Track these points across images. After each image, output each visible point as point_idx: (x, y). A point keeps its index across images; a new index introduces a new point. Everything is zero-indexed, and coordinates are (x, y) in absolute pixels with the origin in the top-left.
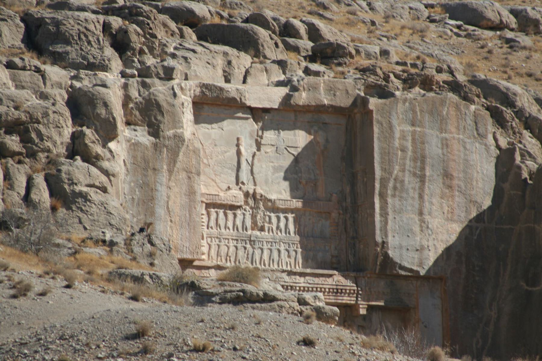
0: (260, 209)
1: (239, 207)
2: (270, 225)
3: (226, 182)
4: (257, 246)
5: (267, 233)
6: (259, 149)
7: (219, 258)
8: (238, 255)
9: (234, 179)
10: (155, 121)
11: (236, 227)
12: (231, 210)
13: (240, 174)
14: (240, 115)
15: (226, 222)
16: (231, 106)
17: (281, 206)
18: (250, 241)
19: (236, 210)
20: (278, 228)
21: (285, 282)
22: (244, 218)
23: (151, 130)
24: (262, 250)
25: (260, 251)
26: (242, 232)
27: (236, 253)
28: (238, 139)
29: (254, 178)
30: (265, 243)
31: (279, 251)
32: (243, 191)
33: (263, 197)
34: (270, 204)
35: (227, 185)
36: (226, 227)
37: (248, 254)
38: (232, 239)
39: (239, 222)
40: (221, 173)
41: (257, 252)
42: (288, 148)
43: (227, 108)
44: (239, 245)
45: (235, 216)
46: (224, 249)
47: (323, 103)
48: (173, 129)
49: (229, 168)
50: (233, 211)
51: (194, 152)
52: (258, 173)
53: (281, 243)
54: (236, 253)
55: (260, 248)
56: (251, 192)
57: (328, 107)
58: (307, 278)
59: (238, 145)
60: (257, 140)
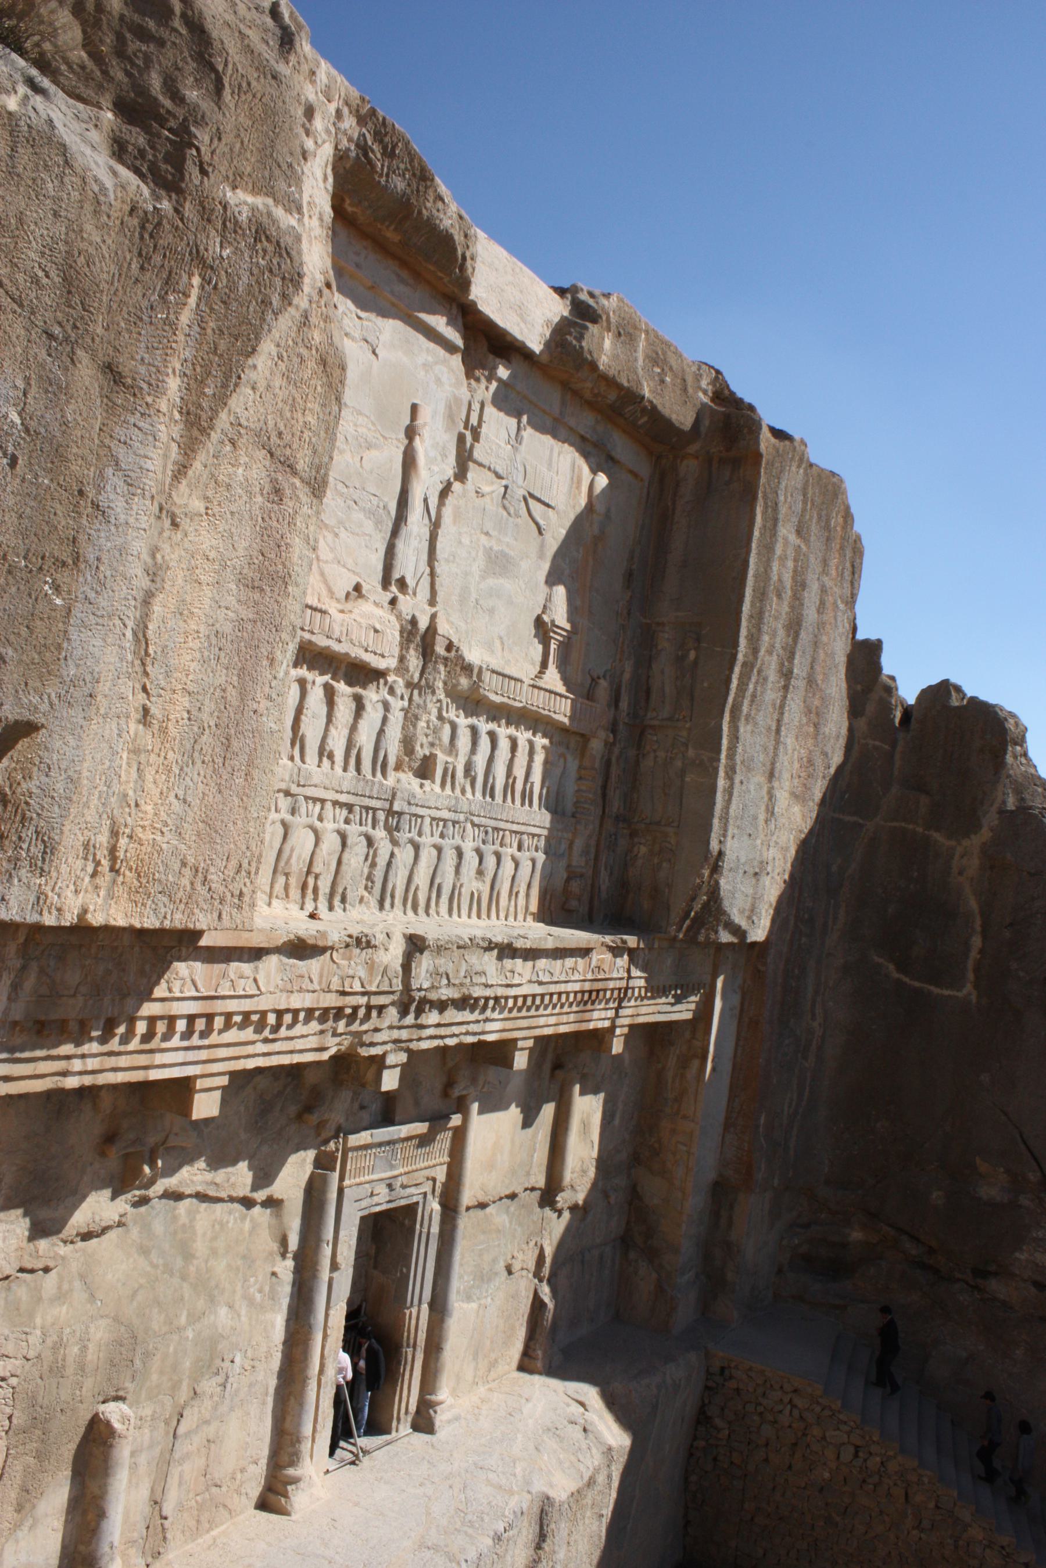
0: (434, 693)
1: (377, 675)
2: (450, 760)
3: (350, 563)
4: (403, 836)
5: (437, 788)
6: (461, 475)
7: (281, 880)
8: (344, 868)
9: (377, 561)
10: (168, 103)
11: (354, 752)
12: (350, 684)
13: (400, 545)
14: (439, 322)
15: (327, 730)
16: (417, 275)
17: (493, 697)
18: (390, 812)
19: (364, 686)
20: (468, 768)
21: (487, 986)
22: (385, 720)
23: (138, 138)
24: (417, 847)
25: (410, 849)
26: (369, 777)
27: (339, 862)
28: (414, 408)
29: (433, 574)
30: (427, 820)
31: (460, 855)
32: (399, 617)
33: (453, 653)
34: (464, 682)
35: (356, 579)
36: (324, 752)
37: (373, 865)
38: (335, 803)
39: (366, 738)
40: (341, 522)
41: (405, 855)
42: (530, 501)
43: (405, 274)
44: (353, 830)
45: (360, 706)
46: (302, 842)
47: (642, 393)
48: (255, 191)
49: (370, 513)
50: (358, 690)
51: (323, 362)
52: (447, 561)
53: (469, 826)
54: (339, 862)
55: (411, 842)
56: (423, 624)
57: (644, 410)
58: (542, 963)
59: (411, 432)
60: (461, 438)
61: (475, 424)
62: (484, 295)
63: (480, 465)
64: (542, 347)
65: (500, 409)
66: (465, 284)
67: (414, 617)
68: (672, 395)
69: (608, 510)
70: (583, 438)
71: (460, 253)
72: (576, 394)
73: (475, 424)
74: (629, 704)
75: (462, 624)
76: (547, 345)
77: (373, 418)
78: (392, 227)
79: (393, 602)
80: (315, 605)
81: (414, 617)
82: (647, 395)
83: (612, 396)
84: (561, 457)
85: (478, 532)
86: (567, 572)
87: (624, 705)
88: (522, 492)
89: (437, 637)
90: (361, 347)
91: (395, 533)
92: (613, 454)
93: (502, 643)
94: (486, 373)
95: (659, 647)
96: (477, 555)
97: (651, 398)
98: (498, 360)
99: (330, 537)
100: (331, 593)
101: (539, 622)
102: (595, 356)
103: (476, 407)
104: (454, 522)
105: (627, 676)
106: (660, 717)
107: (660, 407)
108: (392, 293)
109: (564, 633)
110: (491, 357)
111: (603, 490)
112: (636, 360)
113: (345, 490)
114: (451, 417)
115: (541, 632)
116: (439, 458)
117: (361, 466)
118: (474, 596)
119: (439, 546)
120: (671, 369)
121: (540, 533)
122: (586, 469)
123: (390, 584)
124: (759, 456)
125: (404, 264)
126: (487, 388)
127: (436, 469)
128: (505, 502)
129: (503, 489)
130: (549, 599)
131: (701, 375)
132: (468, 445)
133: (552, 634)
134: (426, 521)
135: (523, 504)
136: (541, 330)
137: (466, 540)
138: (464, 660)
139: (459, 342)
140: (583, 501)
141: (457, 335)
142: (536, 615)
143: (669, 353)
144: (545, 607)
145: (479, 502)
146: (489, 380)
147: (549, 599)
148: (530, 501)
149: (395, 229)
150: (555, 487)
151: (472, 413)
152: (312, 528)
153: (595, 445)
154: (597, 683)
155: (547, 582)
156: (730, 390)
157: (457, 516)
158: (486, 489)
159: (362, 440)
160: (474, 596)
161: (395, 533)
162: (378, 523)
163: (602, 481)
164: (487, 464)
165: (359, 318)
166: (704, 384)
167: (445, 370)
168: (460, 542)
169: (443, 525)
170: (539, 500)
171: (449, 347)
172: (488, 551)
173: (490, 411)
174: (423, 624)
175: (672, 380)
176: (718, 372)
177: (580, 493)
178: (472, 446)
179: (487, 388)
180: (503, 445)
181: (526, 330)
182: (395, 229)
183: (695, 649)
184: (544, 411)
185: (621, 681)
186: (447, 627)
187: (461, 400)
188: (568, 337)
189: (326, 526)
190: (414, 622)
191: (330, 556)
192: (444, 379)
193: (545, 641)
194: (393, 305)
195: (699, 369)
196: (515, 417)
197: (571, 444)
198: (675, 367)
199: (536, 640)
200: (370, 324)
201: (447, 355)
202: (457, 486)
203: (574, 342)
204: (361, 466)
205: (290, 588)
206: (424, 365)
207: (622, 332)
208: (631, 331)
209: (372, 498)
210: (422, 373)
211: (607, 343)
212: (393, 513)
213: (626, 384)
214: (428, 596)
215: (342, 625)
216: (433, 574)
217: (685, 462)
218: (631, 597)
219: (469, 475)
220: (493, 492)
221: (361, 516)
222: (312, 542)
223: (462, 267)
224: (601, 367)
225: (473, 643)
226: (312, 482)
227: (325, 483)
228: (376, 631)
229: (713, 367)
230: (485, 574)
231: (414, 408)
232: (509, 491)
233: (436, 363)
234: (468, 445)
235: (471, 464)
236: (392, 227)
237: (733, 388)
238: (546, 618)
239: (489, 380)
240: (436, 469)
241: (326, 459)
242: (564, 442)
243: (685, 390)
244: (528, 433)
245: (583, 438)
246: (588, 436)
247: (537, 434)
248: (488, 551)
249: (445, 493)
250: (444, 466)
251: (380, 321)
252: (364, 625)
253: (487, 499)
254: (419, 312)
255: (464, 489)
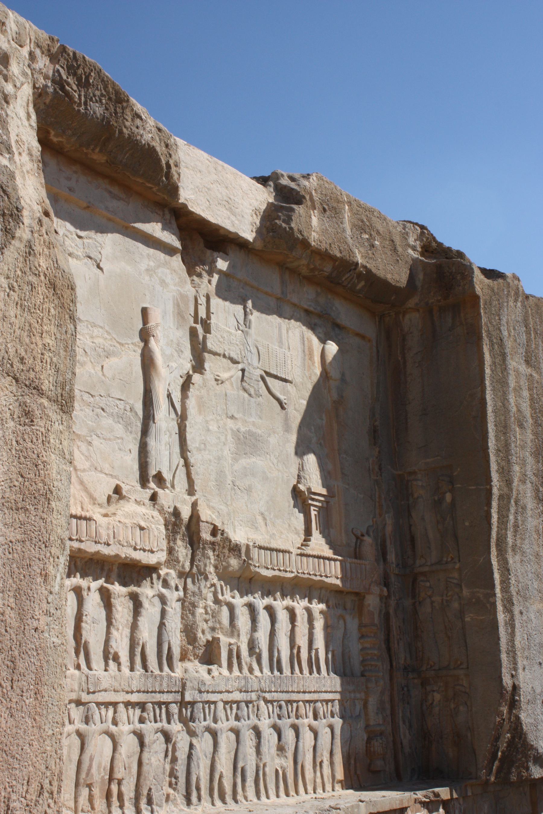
0: (206, 578)
2: (233, 641)
3: (106, 467)
4: (199, 726)
5: (225, 672)
11: (138, 650)
12: (124, 584)
13: (152, 442)
15: (108, 632)
17: (265, 573)
18: (183, 704)
20: (252, 646)
22: (163, 613)
24: (214, 734)
25: (208, 737)
26: (157, 672)
27: (140, 764)
28: (145, 312)
29: (187, 465)
30: (220, 705)
32: (161, 511)
33: (219, 537)
34: (234, 563)
35: (113, 483)
37: (174, 760)
38: (128, 704)
40: (92, 431)
42: (268, 379)
43: (116, 190)
44: (149, 728)
47: (355, 261)
49: (120, 417)
50: (133, 588)
51: (53, 286)
52: (199, 449)
53: (262, 703)
54: (140, 764)
55: (208, 729)
56: (186, 514)
57: (360, 275)
60: (193, 333)
61: (204, 316)
62: (192, 197)
63: (215, 354)
64: (254, 235)
65: (225, 299)
66: (174, 190)
67: (175, 508)
68: (383, 256)
69: (343, 375)
70: (307, 312)
71: (164, 162)
72: (294, 272)
73: (204, 316)
74: (397, 555)
75: (223, 507)
76: (259, 232)
77: (107, 328)
78: (97, 150)
79: (154, 498)
80: (79, 514)
81: (175, 508)
82: (360, 261)
83: (328, 268)
84: (290, 332)
85: (224, 417)
86: (314, 440)
87: (392, 557)
88: (259, 372)
89: (201, 524)
90: (86, 264)
91: (145, 432)
92: (338, 321)
93: (265, 519)
94: (207, 268)
95: (416, 495)
96: (226, 439)
97: (365, 263)
98: (215, 254)
99: (84, 447)
100: (93, 500)
101: (296, 492)
102: (305, 234)
103: (202, 300)
104: (200, 412)
105: (389, 529)
106: (429, 563)
107: (374, 270)
108: (107, 208)
109: (322, 499)
110: (209, 252)
111: (335, 357)
112: (344, 230)
113: (92, 399)
114: (180, 315)
115: (299, 502)
116: (175, 354)
117: (104, 375)
118: (229, 479)
119: (189, 436)
120: (378, 233)
121: (283, 408)
122: (315, 340)
123: (148, 481)
124: (477, 298)
125: (113, 181)
126: (210, 282)
127: (174, 365)
128: (244, 384)
129: (240, 373)
130: (301, 468)
131: (407, 234)
132: (201, 337)
133: (310, 502)
134: (173, 415)
135: (261, 383)
136: (251, 219)
137: (213, 427)
138: (230, 541)
139: (177, 244)
140: (318, 370)
141: (174, 237)
142: (292, 486)
143: (373, 218)
144: (299, 476)
145: (219, 389)
146: (210, 273)
147: (301, 468)
148: (268, 379)
149: (101, 151)
150: (289, 362)
151: (199, 306)
152: (65, 443)
153: (320, 316)
154: (362, 541)
155: (296, 453)
156: (436, 242)
157: (201, 405)
158: (224, 375)
159: (100, 350)
160: (229, 479)
161: (145, 432)
162: (127, 426)
163: (332, 348)
164: (222, 352)
165: (80, 237)
166: (411, 241)
167: (168, 271)
168: (208, 430)
169: (189, 417)
170: (276, 377)
171: (169, 250)
172: (236, 433)
173: (216, 302)
174: (186, 514)
175: (381, 243)
176: (422, 227)
177: (313, 363)
178: (205, 338)
179: (210, 282)
180: (233, 331)
181: (237, 222)
182: (101, 151)
183: (451, 491)
184: (266, 293)
185: (384, 535)
186: (209, 512)
187: (187, 296)
188: (277, 221)
189: (79, 436)
190: (176, 513)
191: (87, 465)
192: (168, 280)
193: (305, 510)
194: (109, 220)
195: (404, 229)
196: (241, 304)
197: (297, 320)
198: (381, 230)
199: (296, 510)
200: (90, 241)
201: (168, 257)
202: (196, 378)
203: (284, 225)
204: (104, 375)
205: (53, 504)
206: (147, 270)
207: (326, 207)
208: (335, 205)
209: (118, 402)
210: (147, 278)
211: (315, 221)
212: (140, 413)
213: (339, 255)
214: (186, 486)
215: (108, 528)
216: (187, 465)
217: (407, 316)
218: (379, 452)
219: (207, 365)
220: (232, 377)
221: (110, 421)
222: (67, 456)
223: (168, 175)
224: (313, 244)
225: (236, 523)
226: (60, 398)
227: (71, 398)
228: (142, 529)
229: (417, 224)
230: (237, 456)
231: (145, 312)
232: (246, 374)
233: (159, 267)
234: (201, 337)
235: (206, 355)
236: (97, 150)
237: (439, 239)
238: (302, 487)
239: (210, 273)
240: (174, 365)
241: (69, 376)
242: (289, 319)
243: (395, 250)
244: (255, 316)
245: (307, 312)
246: (311, 309)
247: (264, 316)
248: (236, 433)
249: (186, 386)
250: (181, 361)
251: (99, 237)
252: (129, 525)
253: (227, 385)
254: (135, 222)
255: (204, 379)
